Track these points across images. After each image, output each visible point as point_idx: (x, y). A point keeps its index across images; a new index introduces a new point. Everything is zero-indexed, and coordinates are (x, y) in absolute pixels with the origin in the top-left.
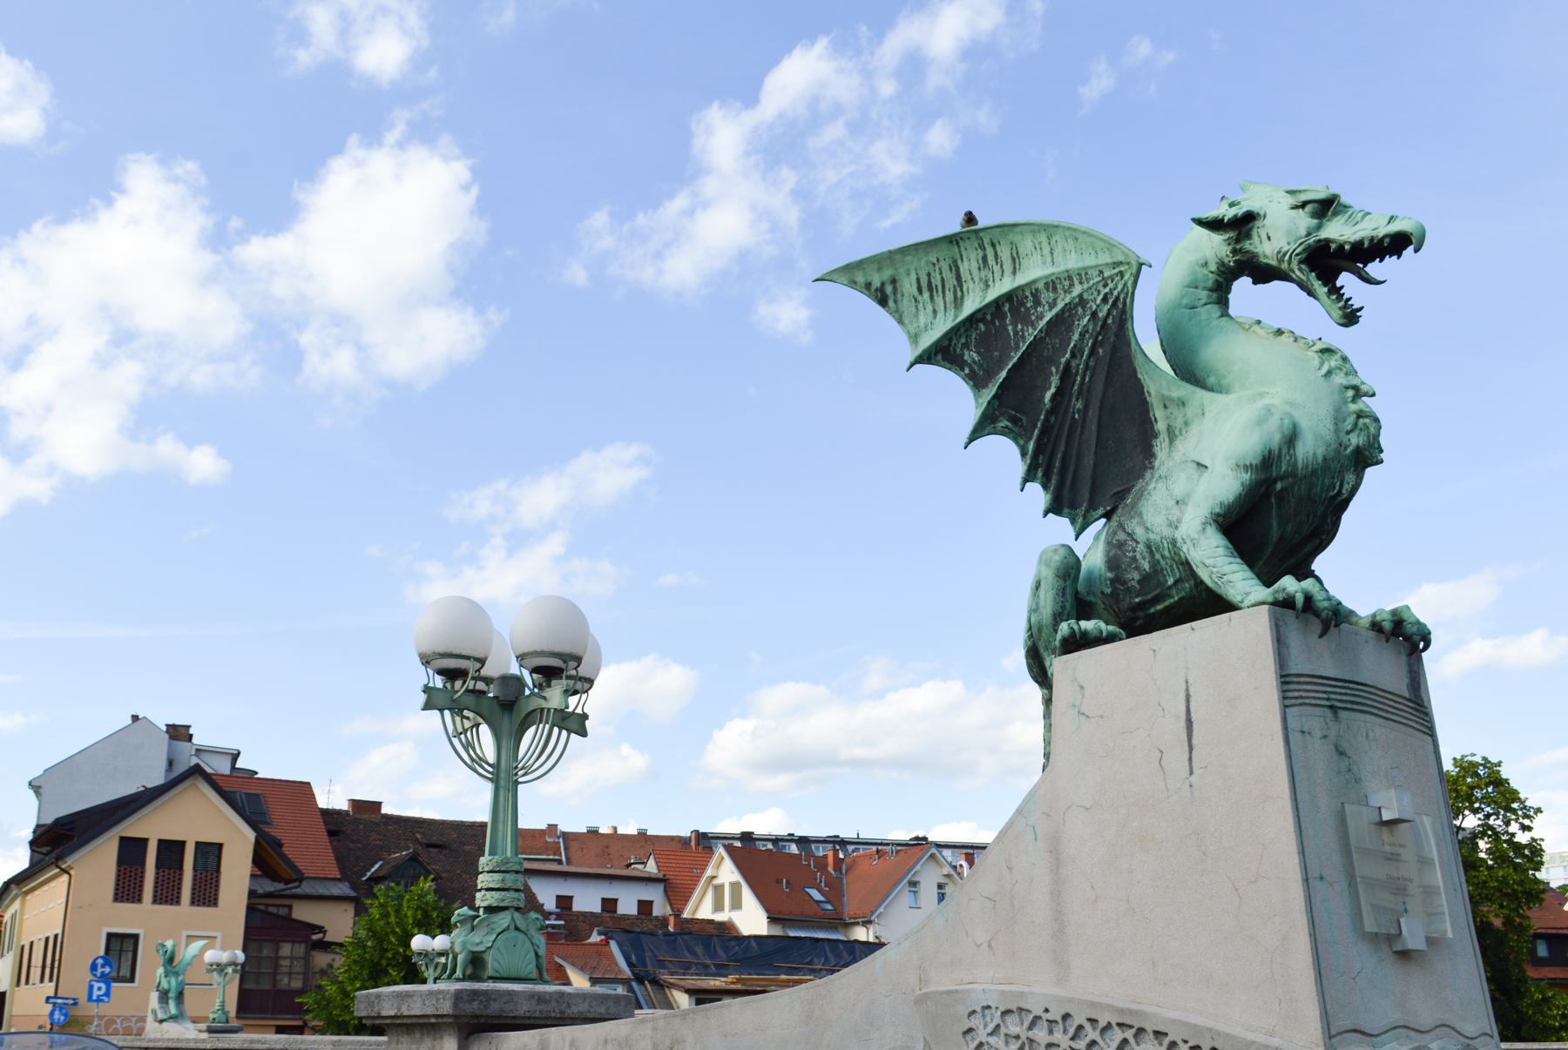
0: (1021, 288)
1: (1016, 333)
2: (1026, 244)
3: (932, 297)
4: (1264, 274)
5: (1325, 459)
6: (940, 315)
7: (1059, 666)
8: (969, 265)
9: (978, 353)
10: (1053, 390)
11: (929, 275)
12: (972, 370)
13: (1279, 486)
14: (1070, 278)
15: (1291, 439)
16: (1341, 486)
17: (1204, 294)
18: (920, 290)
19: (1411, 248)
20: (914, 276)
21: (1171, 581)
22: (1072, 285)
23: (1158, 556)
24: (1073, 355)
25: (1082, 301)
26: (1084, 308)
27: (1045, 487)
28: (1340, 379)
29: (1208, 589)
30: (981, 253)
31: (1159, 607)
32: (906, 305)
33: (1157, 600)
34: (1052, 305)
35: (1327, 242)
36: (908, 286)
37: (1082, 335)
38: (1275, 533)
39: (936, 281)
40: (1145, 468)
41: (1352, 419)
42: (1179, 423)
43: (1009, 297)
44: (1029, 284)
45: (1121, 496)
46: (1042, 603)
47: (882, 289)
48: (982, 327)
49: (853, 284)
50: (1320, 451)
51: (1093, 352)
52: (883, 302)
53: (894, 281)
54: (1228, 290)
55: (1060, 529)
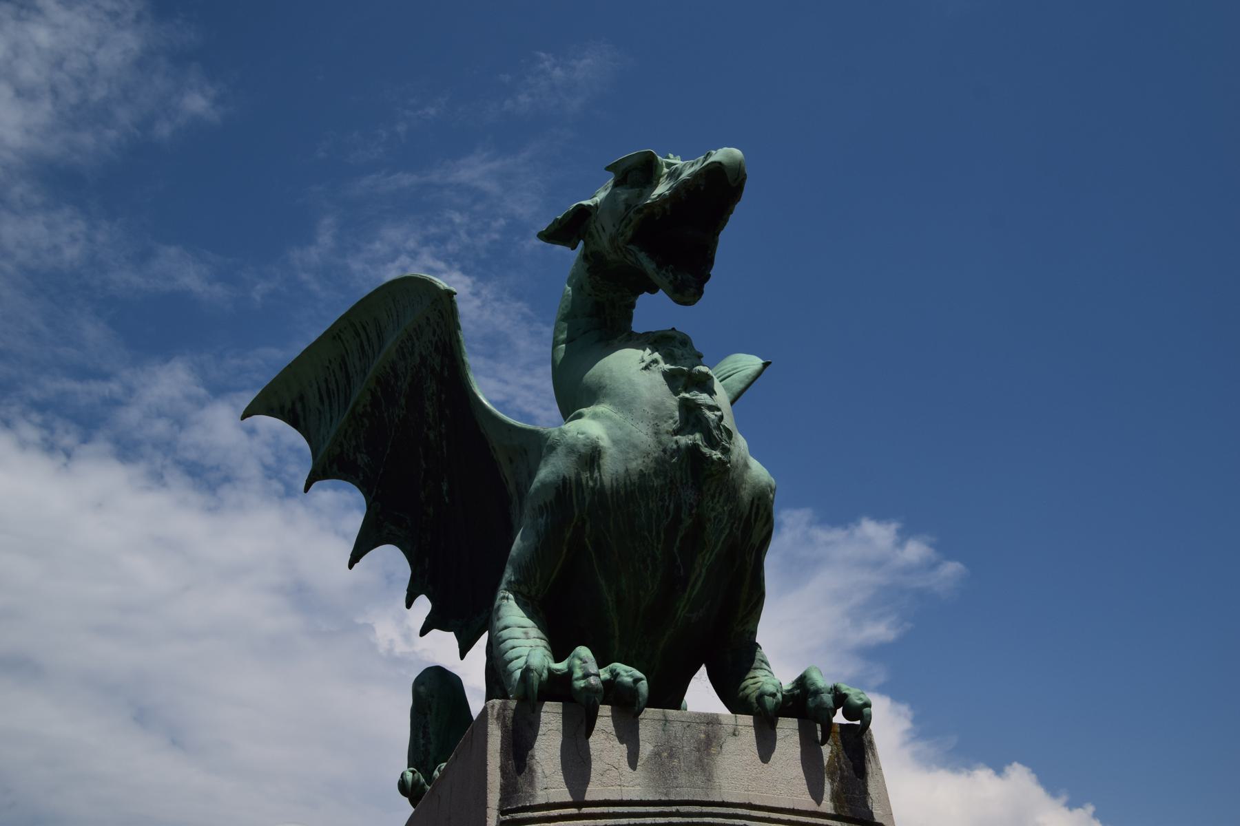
3: (331, 405)
47: (293, 410)
48: (366, 421)
49: (270, 412)
50: (636, 465)
53: (301, 398)
55: (441, 648)
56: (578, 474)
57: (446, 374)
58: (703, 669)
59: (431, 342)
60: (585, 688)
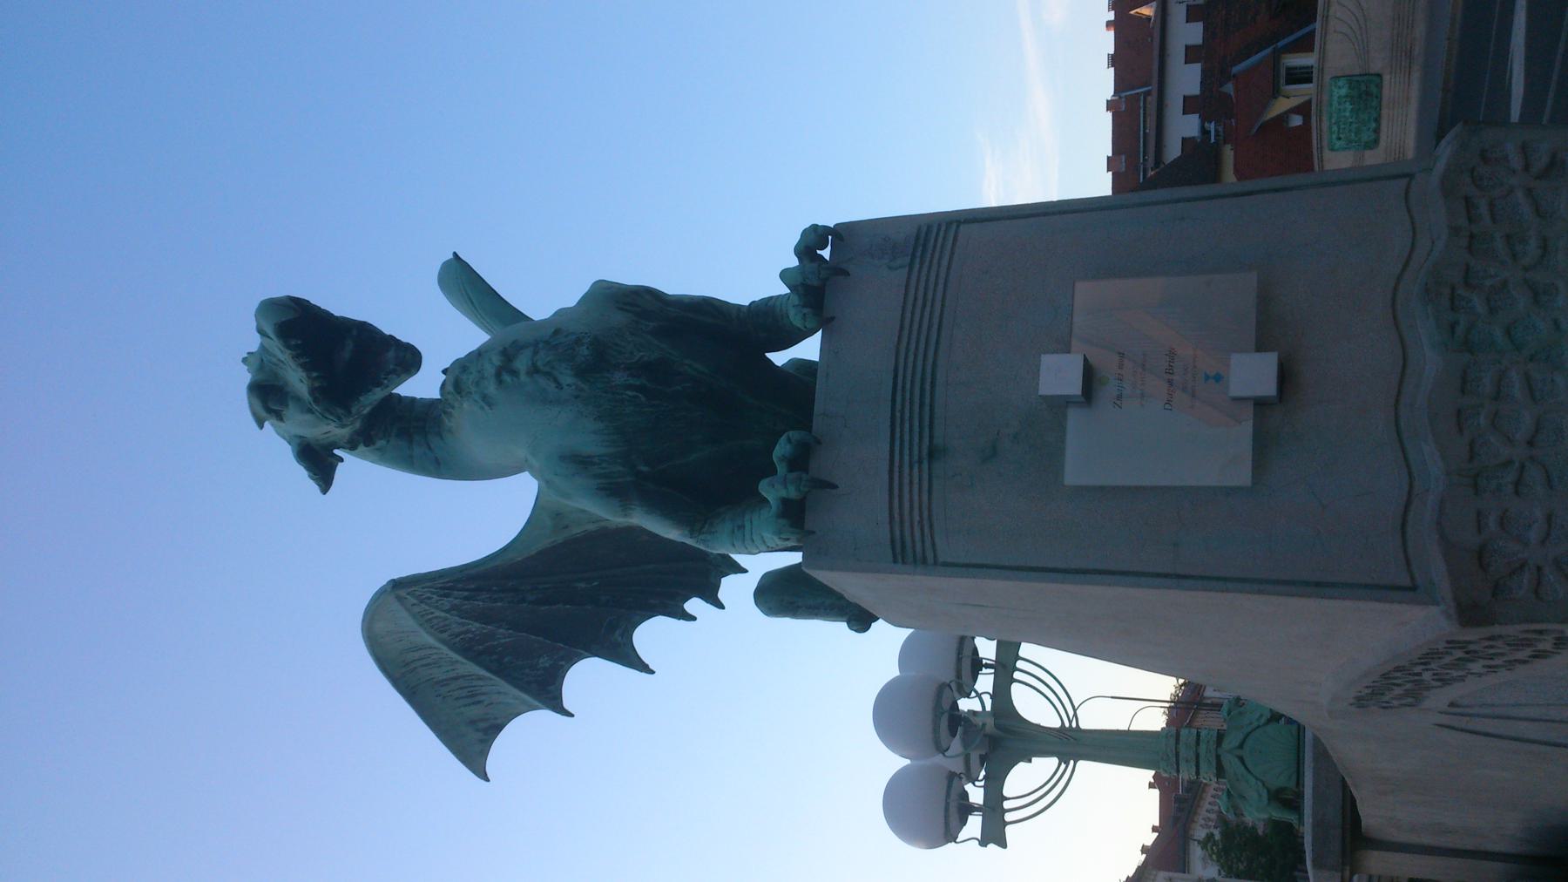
8: (439, 674)
12: (562, 658)
13: (644, 469)
16: (630, 387)
28: (491, 388)
35: (312, 391)
36: (474, 712)
37: (495, 601)
39: (464, 693)
41: (543, 381)
49: (484, 753)
53: (472, 722)
55: (737, 590)
56: (596, 476)
58: (768, 355)
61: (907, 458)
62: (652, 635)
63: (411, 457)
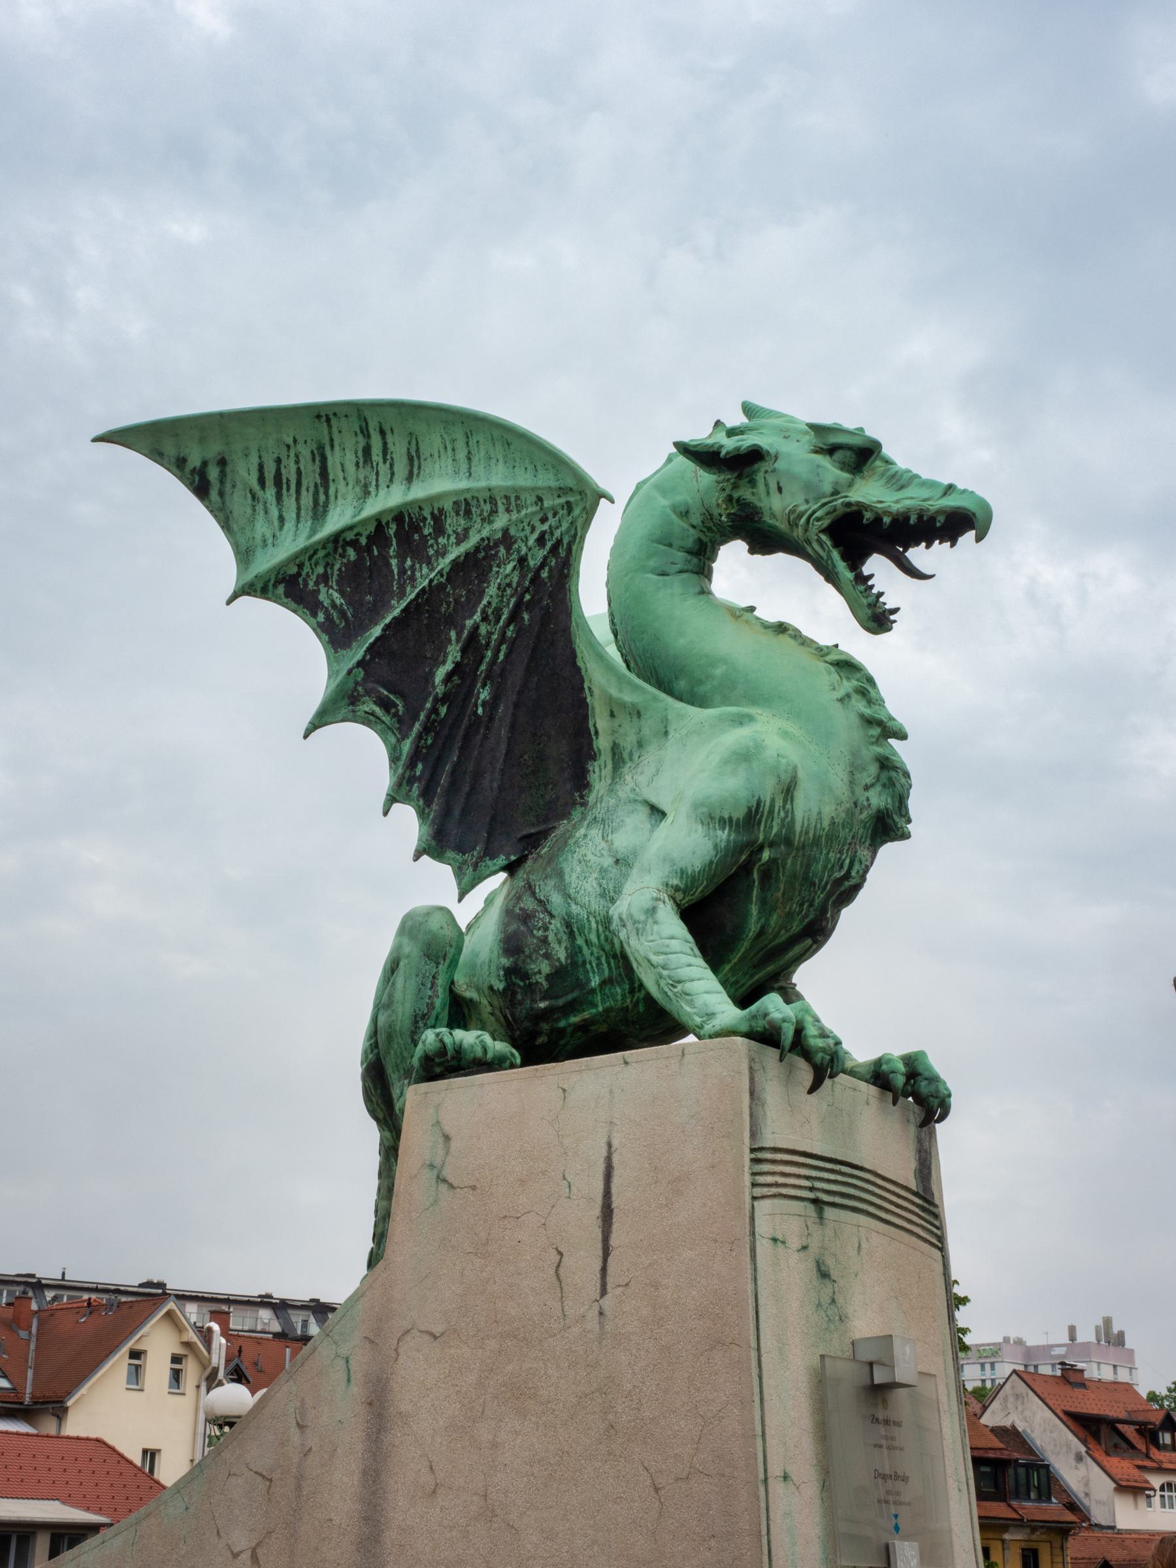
0: (419, 505)
1: (402, 571)
2: (432, 441)
3: (279, 497)
4: (765, 540)
5: (833, 823)
6: (289, 525)
7: (415, 1099)
8: (343, 459)
9: (342, 592)
10: (449, 666)
11: (278, 461)
12: (328, 618)
13: (766, 855)
14: (492, 501)
15: (788, 790)
17: (680, 556)
18: (262, 481)
19: (971, 535)
20: (255, 460)
21: (595, 982)
22: (494, 512)
23: (580, 941)
24: (485, 618)
25: (507, 539)
26: (508, 549)
27: (422, 814)
29: (649, 1000)
30: (362, 442)
31: (574, 1019)
32: (238, 503)
33: (572, 1007)
34: (461, 538)
36: (245, 472)
38: (753, 927)
39: (289, 472)
40: (574, 804)
41: (873, 769)
42: (628, 742)
43: (399, 516)
44: (431, 500)
45: (532, 842)
46: (398, 995)
48: (352, 554)
49: (157, 455)
50: (829, 811)
51: (514, 617)
52: (201, 490)
53: (222, 462)
54: (713, 557)
57: (545, 574)
59: (533, 529)
60: (823, 1050)
61: (814, 1173)
62: (364, 754)
63: (670, 545)
